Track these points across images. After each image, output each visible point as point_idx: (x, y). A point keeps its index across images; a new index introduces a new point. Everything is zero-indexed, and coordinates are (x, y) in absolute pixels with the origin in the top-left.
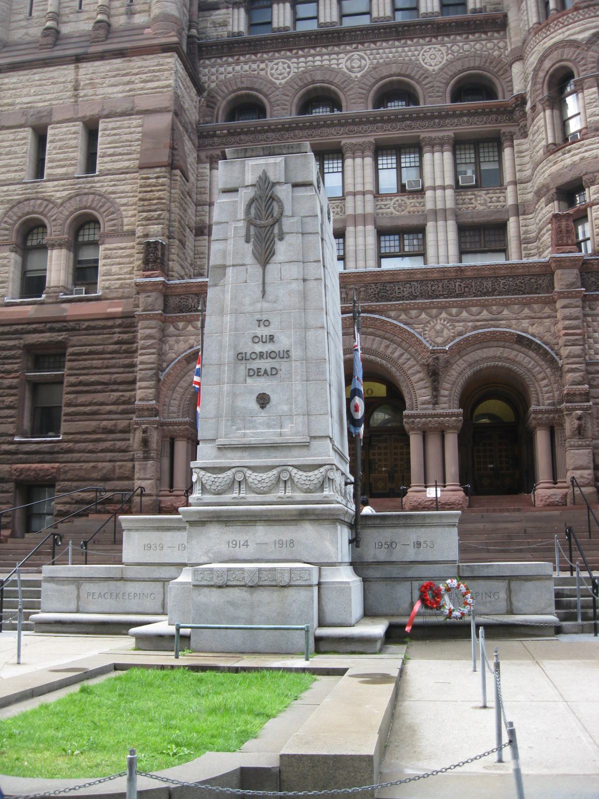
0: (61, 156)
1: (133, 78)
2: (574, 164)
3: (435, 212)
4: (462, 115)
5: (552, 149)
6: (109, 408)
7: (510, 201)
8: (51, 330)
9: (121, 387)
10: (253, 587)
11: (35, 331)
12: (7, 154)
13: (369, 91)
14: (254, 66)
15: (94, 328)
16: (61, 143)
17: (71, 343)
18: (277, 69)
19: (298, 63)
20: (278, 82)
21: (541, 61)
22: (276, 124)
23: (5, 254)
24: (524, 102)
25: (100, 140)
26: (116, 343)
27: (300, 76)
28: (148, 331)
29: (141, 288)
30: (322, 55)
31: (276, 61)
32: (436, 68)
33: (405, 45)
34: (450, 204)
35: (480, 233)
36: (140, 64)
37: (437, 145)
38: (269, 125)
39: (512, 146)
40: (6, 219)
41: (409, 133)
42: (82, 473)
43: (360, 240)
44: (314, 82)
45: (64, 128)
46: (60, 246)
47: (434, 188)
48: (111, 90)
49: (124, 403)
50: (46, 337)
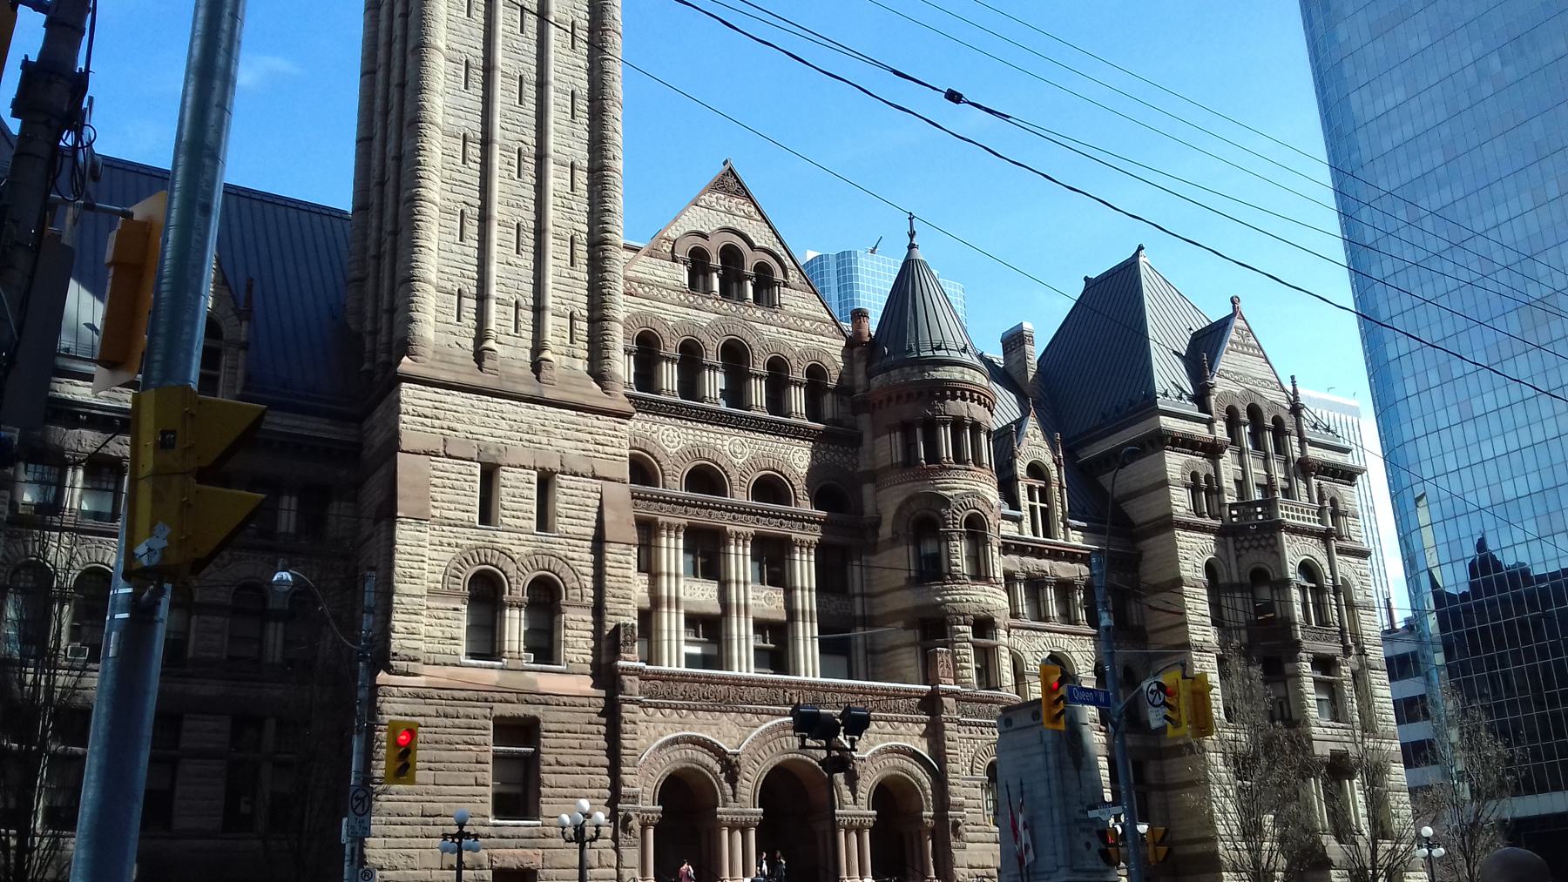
1: (589, 437)
7: (858, 612)
21: (909, 500)
24: (877, 524)
27: (695, 452)
36: (596, 422)
41: (783, 531)
44: (701, 458)
45: (521, 474)
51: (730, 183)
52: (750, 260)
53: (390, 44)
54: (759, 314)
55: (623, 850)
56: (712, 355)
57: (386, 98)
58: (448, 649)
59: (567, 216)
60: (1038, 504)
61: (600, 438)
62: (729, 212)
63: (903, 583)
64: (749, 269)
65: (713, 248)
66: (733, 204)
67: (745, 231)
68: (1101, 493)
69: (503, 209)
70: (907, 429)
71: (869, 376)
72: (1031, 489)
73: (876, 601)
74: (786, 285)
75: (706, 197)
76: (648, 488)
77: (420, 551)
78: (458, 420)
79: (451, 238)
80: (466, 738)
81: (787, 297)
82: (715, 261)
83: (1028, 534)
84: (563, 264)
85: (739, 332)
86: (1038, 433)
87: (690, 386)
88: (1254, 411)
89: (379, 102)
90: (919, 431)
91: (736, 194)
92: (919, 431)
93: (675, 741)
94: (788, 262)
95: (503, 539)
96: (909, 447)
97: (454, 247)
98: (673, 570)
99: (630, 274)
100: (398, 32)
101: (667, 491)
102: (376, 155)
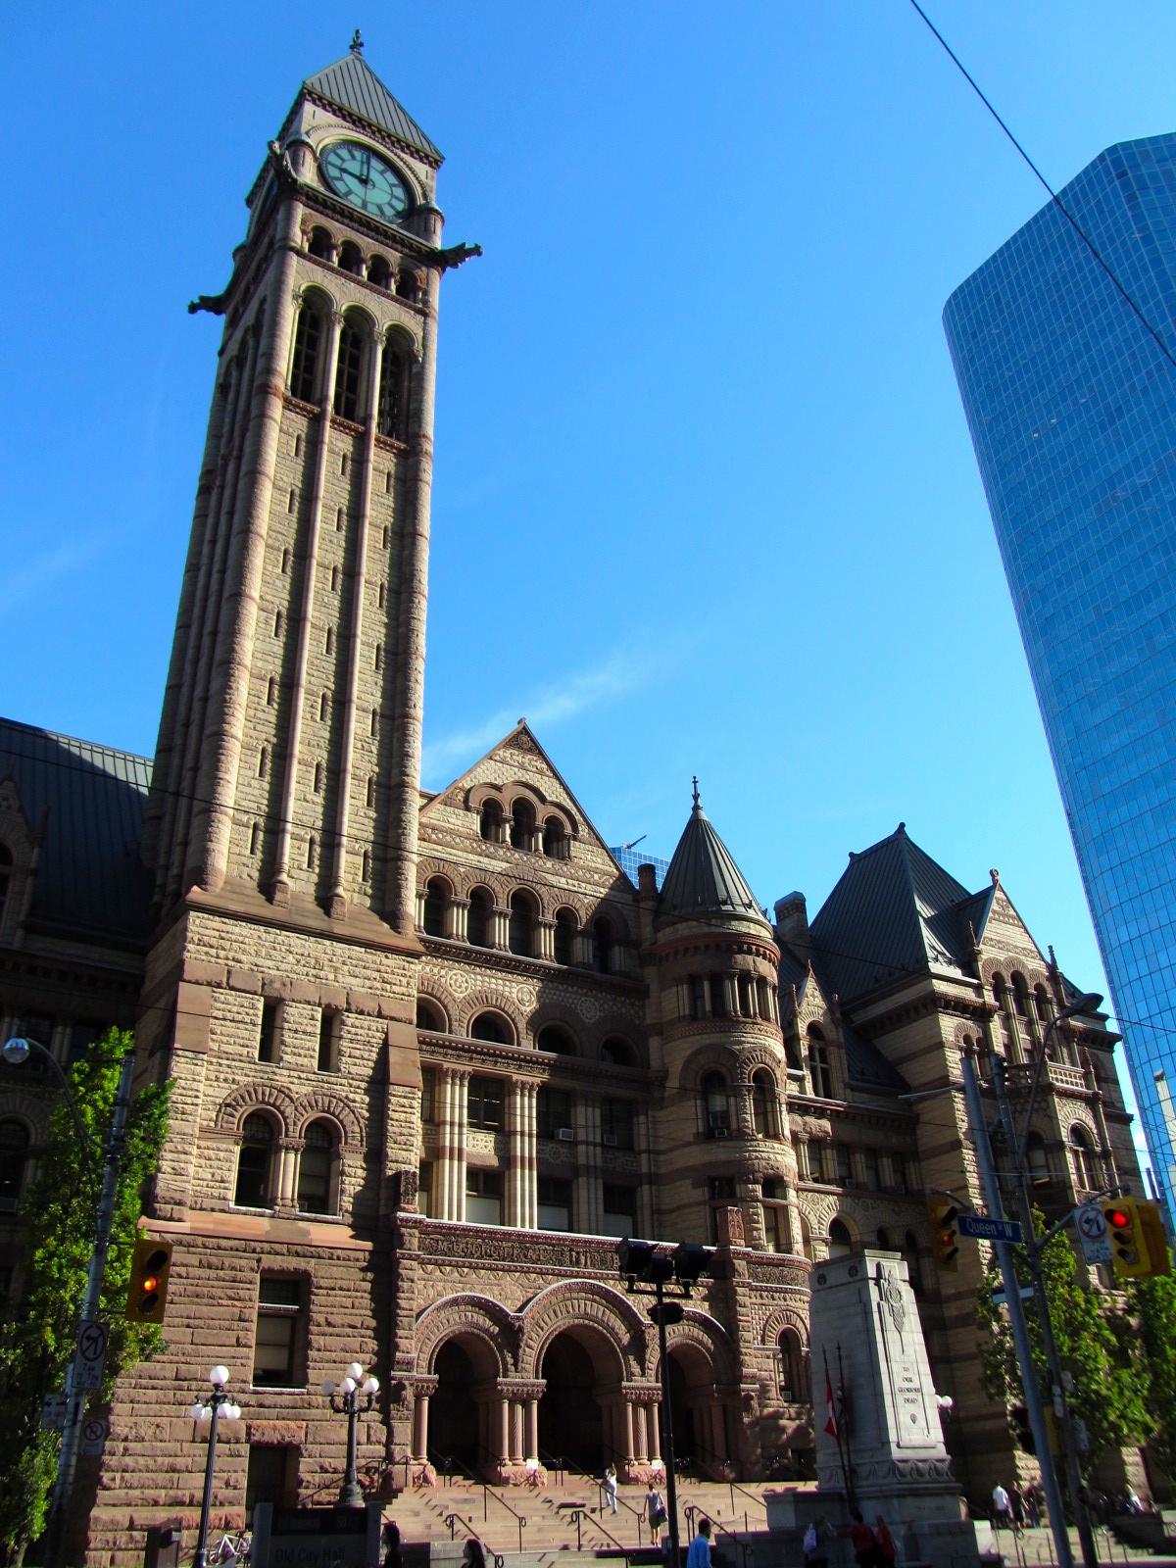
1: (376, 975)
7: (645, 1170)
13: (496, 1007)
14: (436, 970)
18: (456, 980)
19: (476, 980)
20: (456, 995)
21: (698, 1052)
22: (457, 1043)
24: (665, 1078)
27: (482, 998)
30: (496, 978)
31: (455, 972)
32: (592, 1021)
33: (566, 991)
34: (599, 1163)
38: (451, 1042)
39: (647, 1115)
47: (587, 1143)
51: (523, 740)
52: (542, 813)
53: (206, 599)
54: (549, 865)
55: (395, 1423)
56: (502, 904)
57: (198, 648)
59: (361, 760)
60: (819, 1065)
62: (522, 767)
63: (691, 1138)
64: (540, 822)
65: (506, 800)
66: (526, 760)
67: (537, 785)
68: (877, 1055)
69: (305, 749)
70: (693, 981)
71: (656, 930)
73: (663, 1158)
74: (575, 839)
75: (501, 752)
78: (244, 952)
79: (250, 773)
80: (230, 1292)
81: (576, 848)
83: (810, 1094)
84: (359, 803)
86: (817, 993)
87: (479, 932)
88: (1018, 977)
89: (190, 652)
91: (530, 750)
92: (706, 985)
93: (455, 1302)
94: (578, 817)
95: (282, 1078)
96: (696, 998)
98: (457, 1120)
99: (424, 820)
100: (214, 586)
101: (452, 1037)
102: (184, 699)
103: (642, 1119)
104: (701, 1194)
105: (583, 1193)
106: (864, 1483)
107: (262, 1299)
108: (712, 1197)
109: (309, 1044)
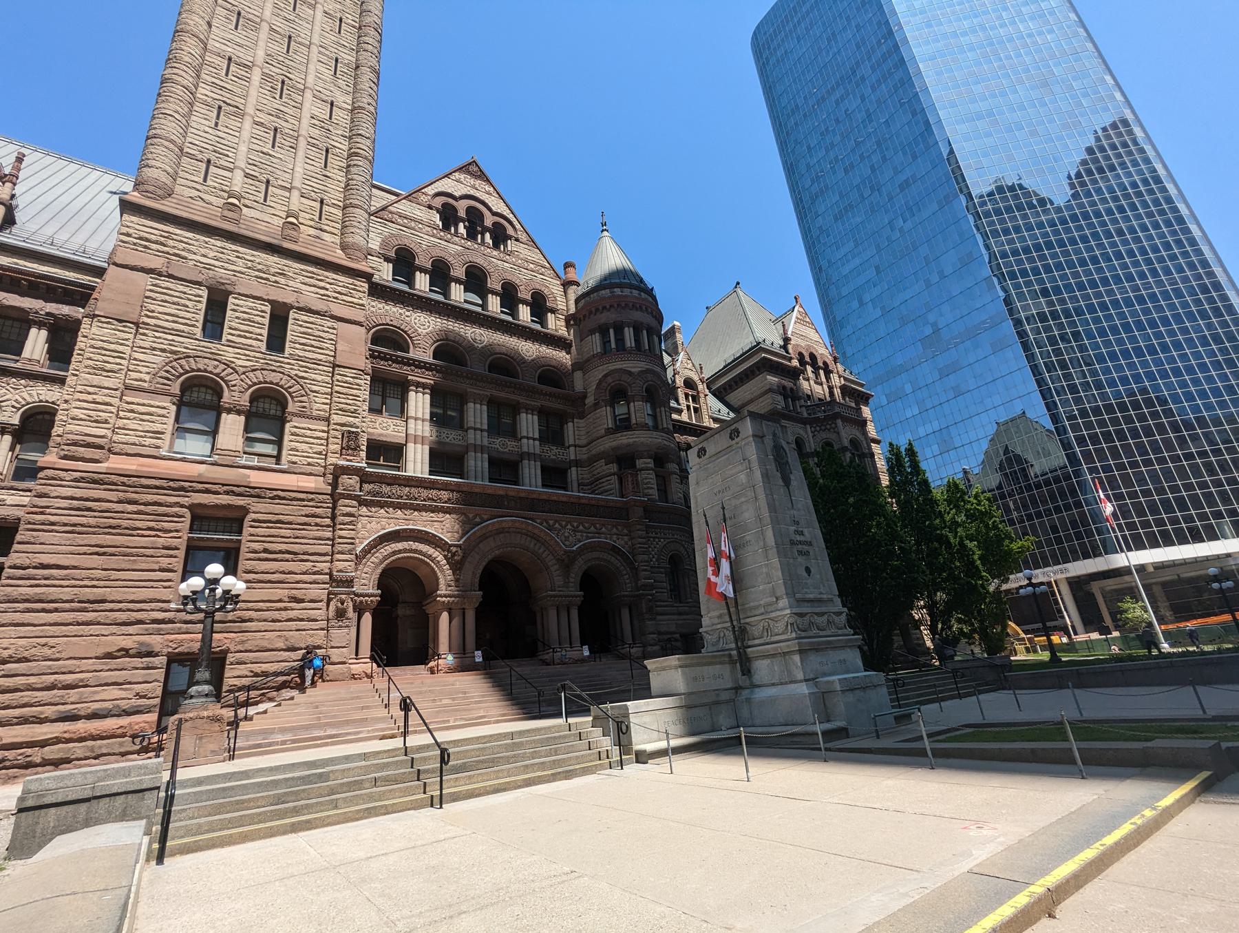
0: (246, 328)
1: (328, 286)
2: (628, 445)
3: (529, 454)
4: (546, 394)
5: (609, 432)
6: (299, 577)
7: (573, 457)
8: (227, 493)
9: (311, 558)
10: (864, 689)
11: (207, 491)
12: (174, 303)
15: (284, 498)
16: (246, 316)
17: (253, 509)
21: (606, 376)
23: (165, 405)
24: (585, 396)
25: (290, 327)
26: (307, 516)
28: (349, 509)
29: (339, 472)
35: (554, 474)
37: (528, 409)
40: (167, 368)
42: (266, 644)
43: (479, 463)
46: (239, 413)
47: (528, 438)
48: (304, 287)
49: (314, 573)
50: (224, 499)
52: (489, 221)
54: (495, 253)
58: (148, 441)
61: (339, 289)
62: (474, 187)
70: (603, 331)
72: (687, 395)
74: (517, 240)
76: (399, 353)
77: (121, 348)
78: (189, 251)
82: (462, 213)
85: (480, 261)
88: (812, 356)
90: (612, 331)
92: (612, 331)
95: (229, 354)
96: (605, 342)
97: (210, 130)
101: (416, 357)
103: (570, 424)
104: (614, 468)
105: (526, 471)
106: (757, 642)
107: (191, 530)
108: (620, 469)
109: (259, 331)
